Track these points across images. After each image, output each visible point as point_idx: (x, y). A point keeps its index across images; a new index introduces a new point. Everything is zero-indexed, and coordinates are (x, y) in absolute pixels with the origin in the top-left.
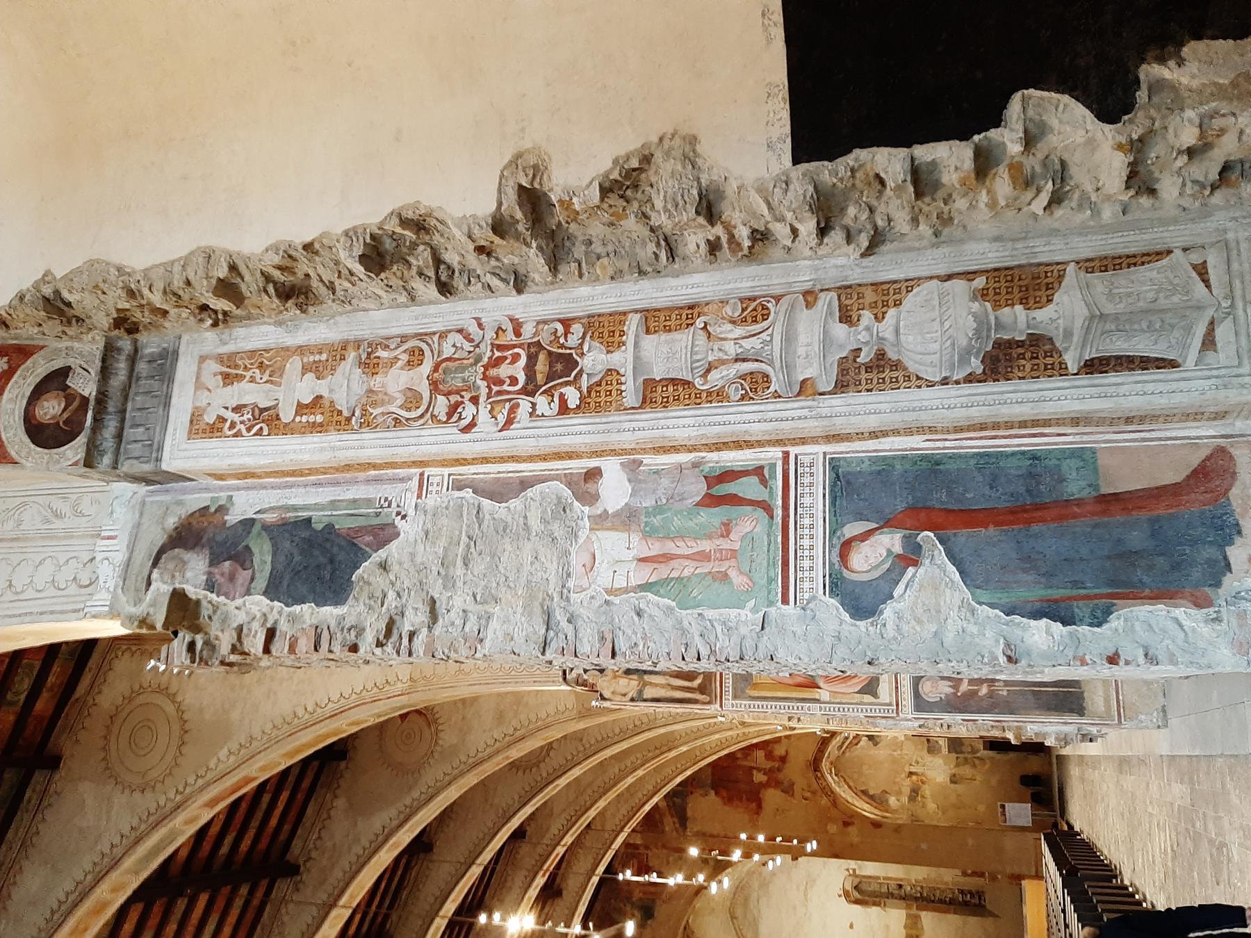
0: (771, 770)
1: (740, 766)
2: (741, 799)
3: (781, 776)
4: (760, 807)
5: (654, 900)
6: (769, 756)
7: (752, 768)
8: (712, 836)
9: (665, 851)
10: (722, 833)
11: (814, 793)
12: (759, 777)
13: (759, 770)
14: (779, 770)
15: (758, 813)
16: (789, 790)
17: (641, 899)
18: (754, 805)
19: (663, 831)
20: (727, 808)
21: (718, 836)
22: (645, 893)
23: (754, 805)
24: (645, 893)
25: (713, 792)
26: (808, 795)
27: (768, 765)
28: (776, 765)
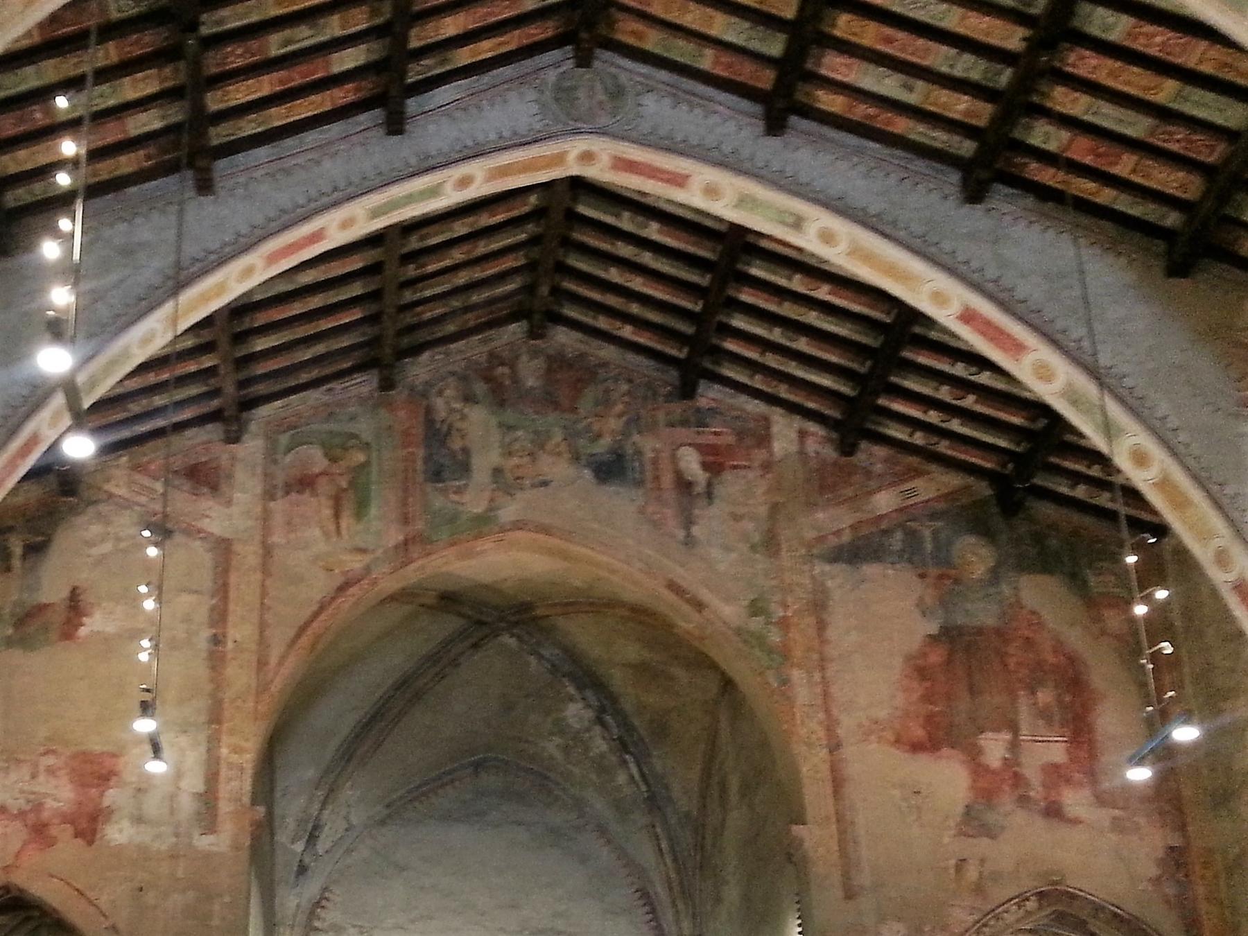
0: (1018, 780)
1: (1014, 700)
2: (927, 698)
3: (1006, 801)
4: (916, 747)
5: (639, 483)
6: (1055, 774)
7: (1014, 728)
8: (821, 626)
9: (763, 510)
10: (831, 651)
11: (979, 889)
12: (994, 748)
13: (1014, 746)
14: (1023, 801)
15: (898, 741)
16: (974, 822)
17: (639, 453)
18: (919, 733)
19: (811, 506)
20: (898, 662)
21: (824, 642)
22: (655, 462)
23: (919, 733)
24: (655, 462)
25: (933, 628)
26: (972, 874)
27: (1031, 769)
28: (1036, 792)
